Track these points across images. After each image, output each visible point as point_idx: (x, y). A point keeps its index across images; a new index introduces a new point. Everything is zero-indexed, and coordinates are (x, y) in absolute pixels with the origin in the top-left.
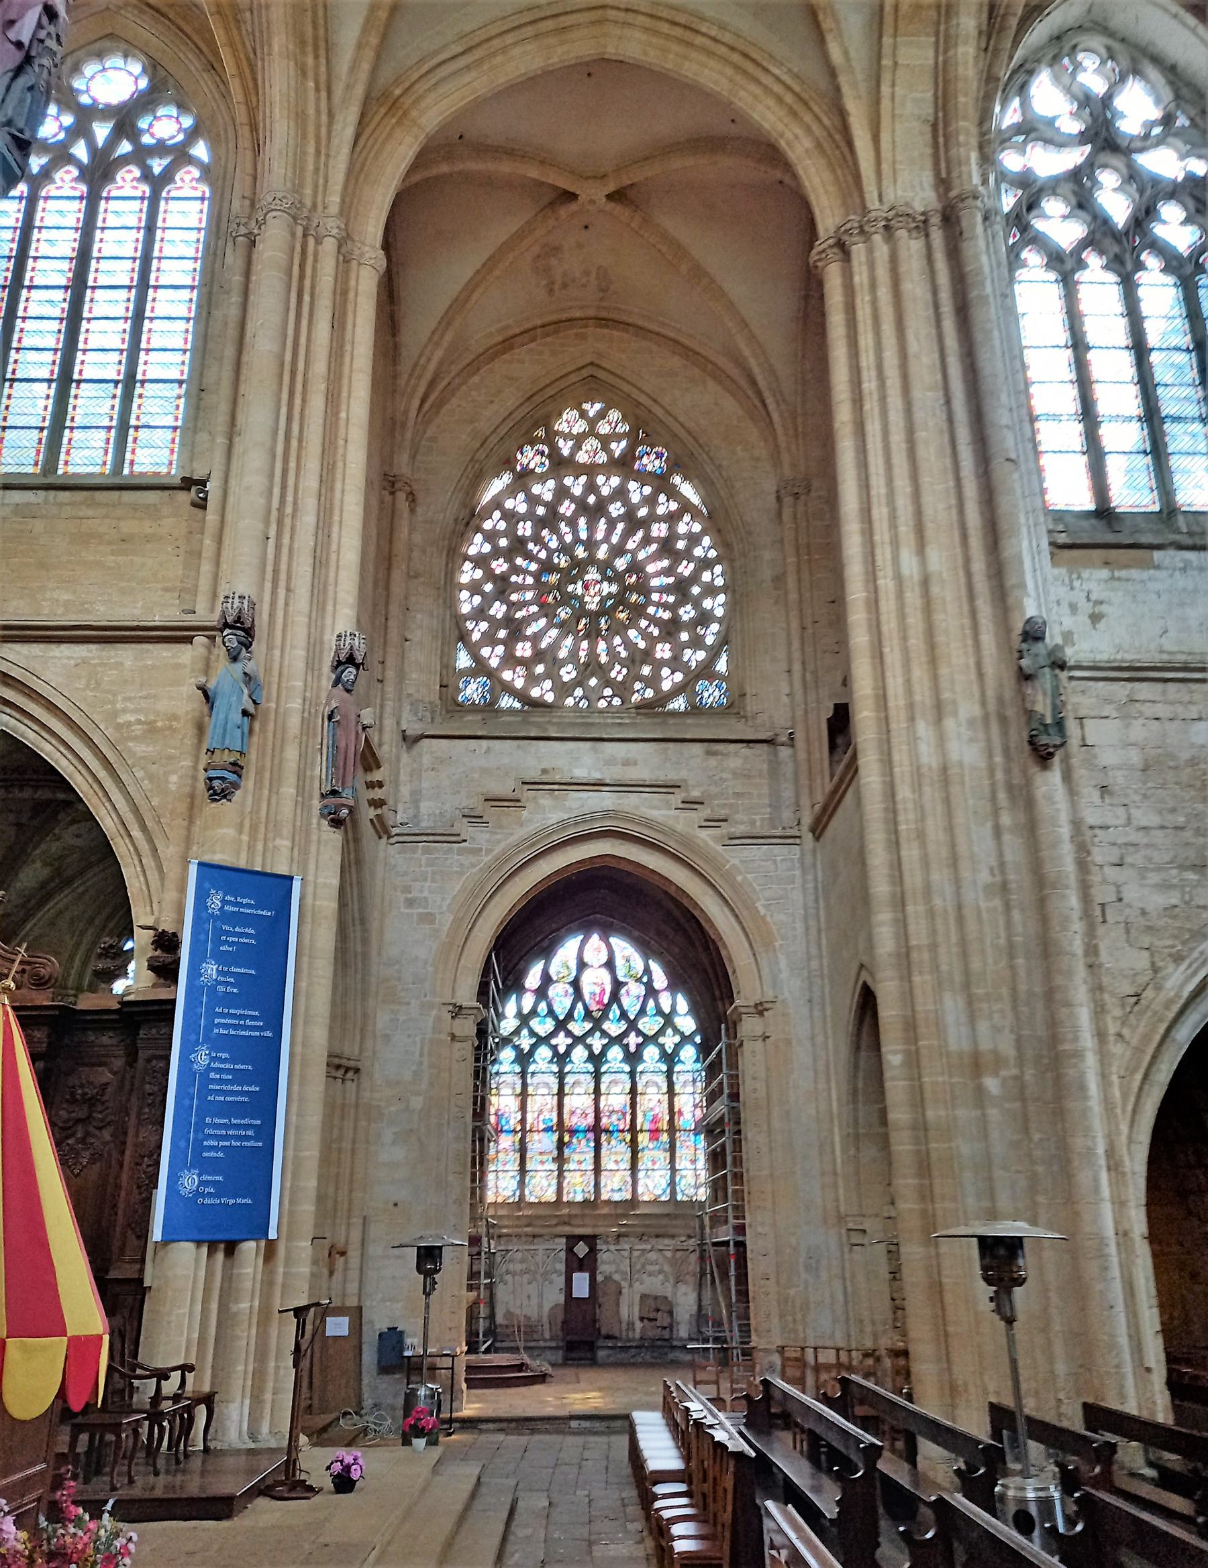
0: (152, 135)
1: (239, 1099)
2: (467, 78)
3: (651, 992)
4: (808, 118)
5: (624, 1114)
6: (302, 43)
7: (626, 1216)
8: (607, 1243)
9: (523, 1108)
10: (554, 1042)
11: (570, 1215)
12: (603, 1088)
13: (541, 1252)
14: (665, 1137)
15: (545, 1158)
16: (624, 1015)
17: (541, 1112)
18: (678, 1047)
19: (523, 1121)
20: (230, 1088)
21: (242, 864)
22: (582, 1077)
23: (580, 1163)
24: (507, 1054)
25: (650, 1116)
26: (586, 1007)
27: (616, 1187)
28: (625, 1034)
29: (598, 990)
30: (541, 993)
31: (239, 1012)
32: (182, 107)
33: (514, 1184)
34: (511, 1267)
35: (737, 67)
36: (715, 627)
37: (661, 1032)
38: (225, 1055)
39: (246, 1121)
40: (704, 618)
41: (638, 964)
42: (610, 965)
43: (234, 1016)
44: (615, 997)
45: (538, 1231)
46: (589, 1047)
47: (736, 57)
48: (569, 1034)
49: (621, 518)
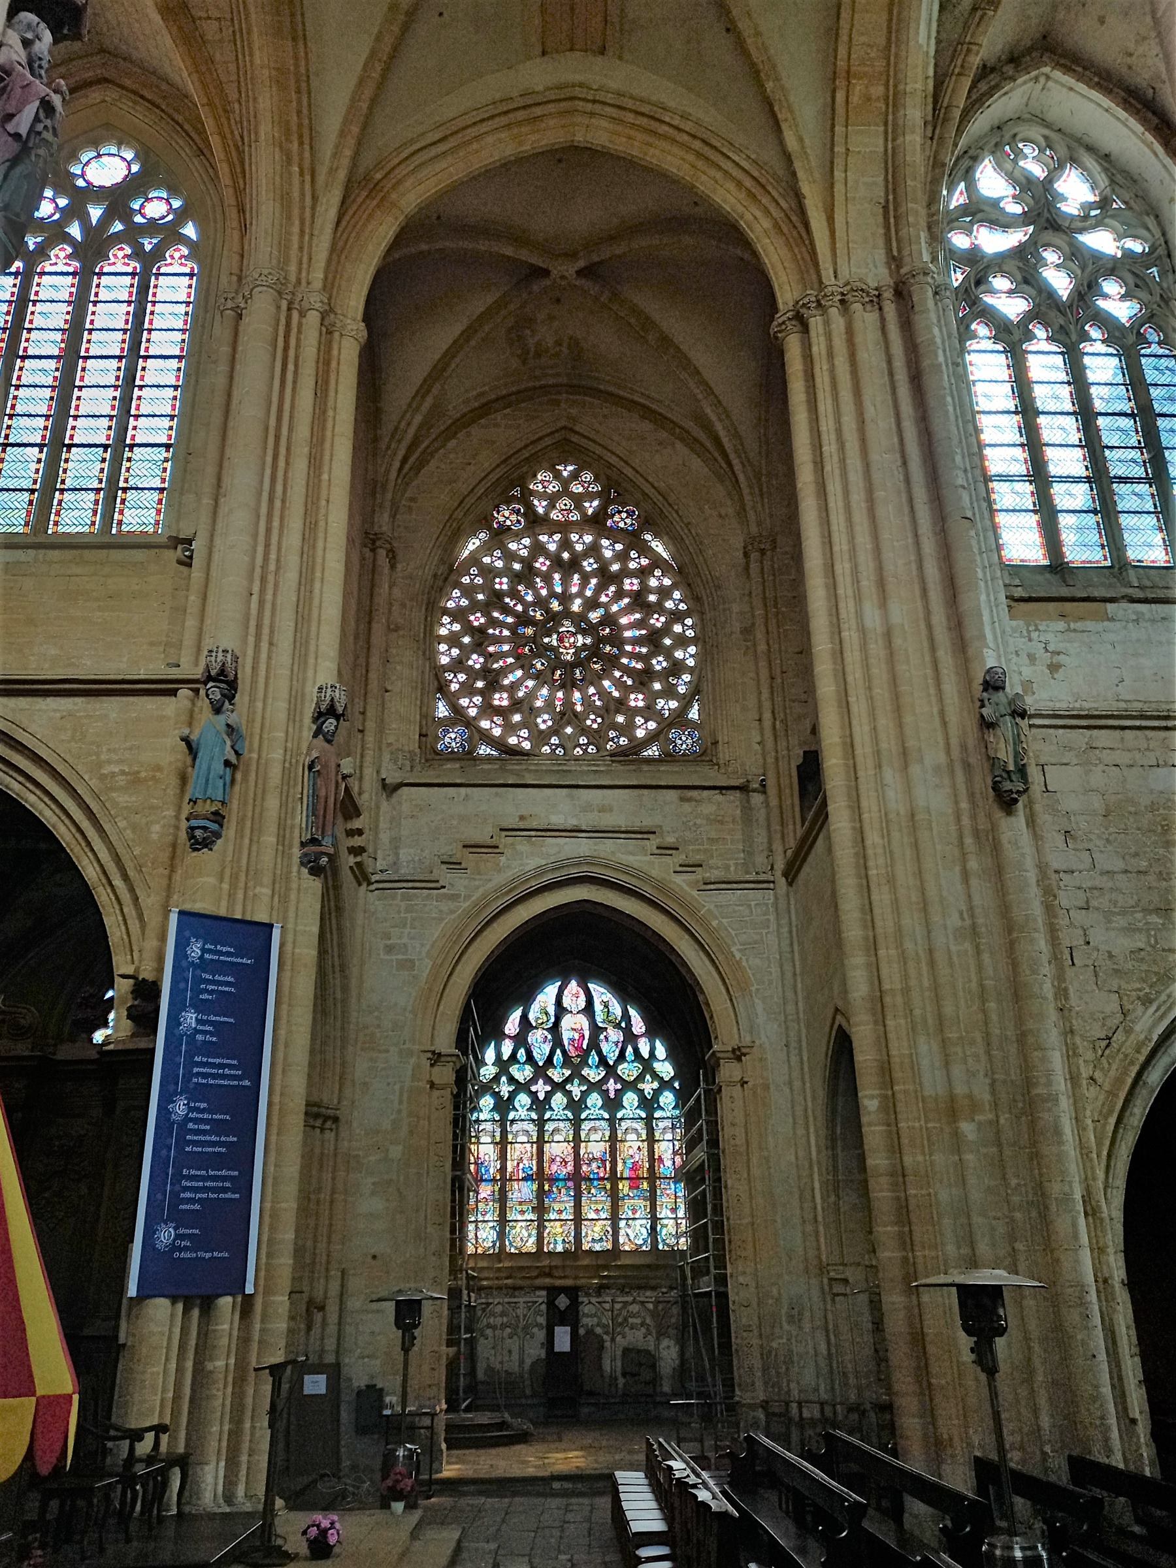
0: (144, 216)
1: (217, 1149)
2: (444, 165)
3: (630, 1037)
4: (765, 200)
5: (604, 1162)
6: (287, 132)
7: (606, 1267)
8: (588, 1295)
9: (503, 1157)
10: (533, 1089)
11: (550, 1267)
12: (583, 1135)
13: (521, 1305)
14: (645, 1185)
15: (525, 1208)
16: (603, 1061)
18: (657, 1093)
19: (503, 1169)
20: (208, 1138)
21: (222, 912)
22: (561, 1125)
23: (560, 1212)
24: (487, 1102)
26: (564, 1052)
27: (597, 1237)
28: (604, 1080)
29: (577, 1036)
30: (520, 1040)
31: (217, 1061)
32: (173, 191)
33: (493, 1235)
34: (491, 1320)
35: (699, 155)
36: (686, 677)
37: (640, 1078)
38: (203, 1105)
39: (224, 1173)
40: (676, 668)
41: (617, 1010)
42: (589, 1009)
43: (213, 1065)
44: (594, 1044)
45: (520, 1282)
46: (568, 1094)
47: (697, 145)
48: (548, 1080)
49: (594, 573)
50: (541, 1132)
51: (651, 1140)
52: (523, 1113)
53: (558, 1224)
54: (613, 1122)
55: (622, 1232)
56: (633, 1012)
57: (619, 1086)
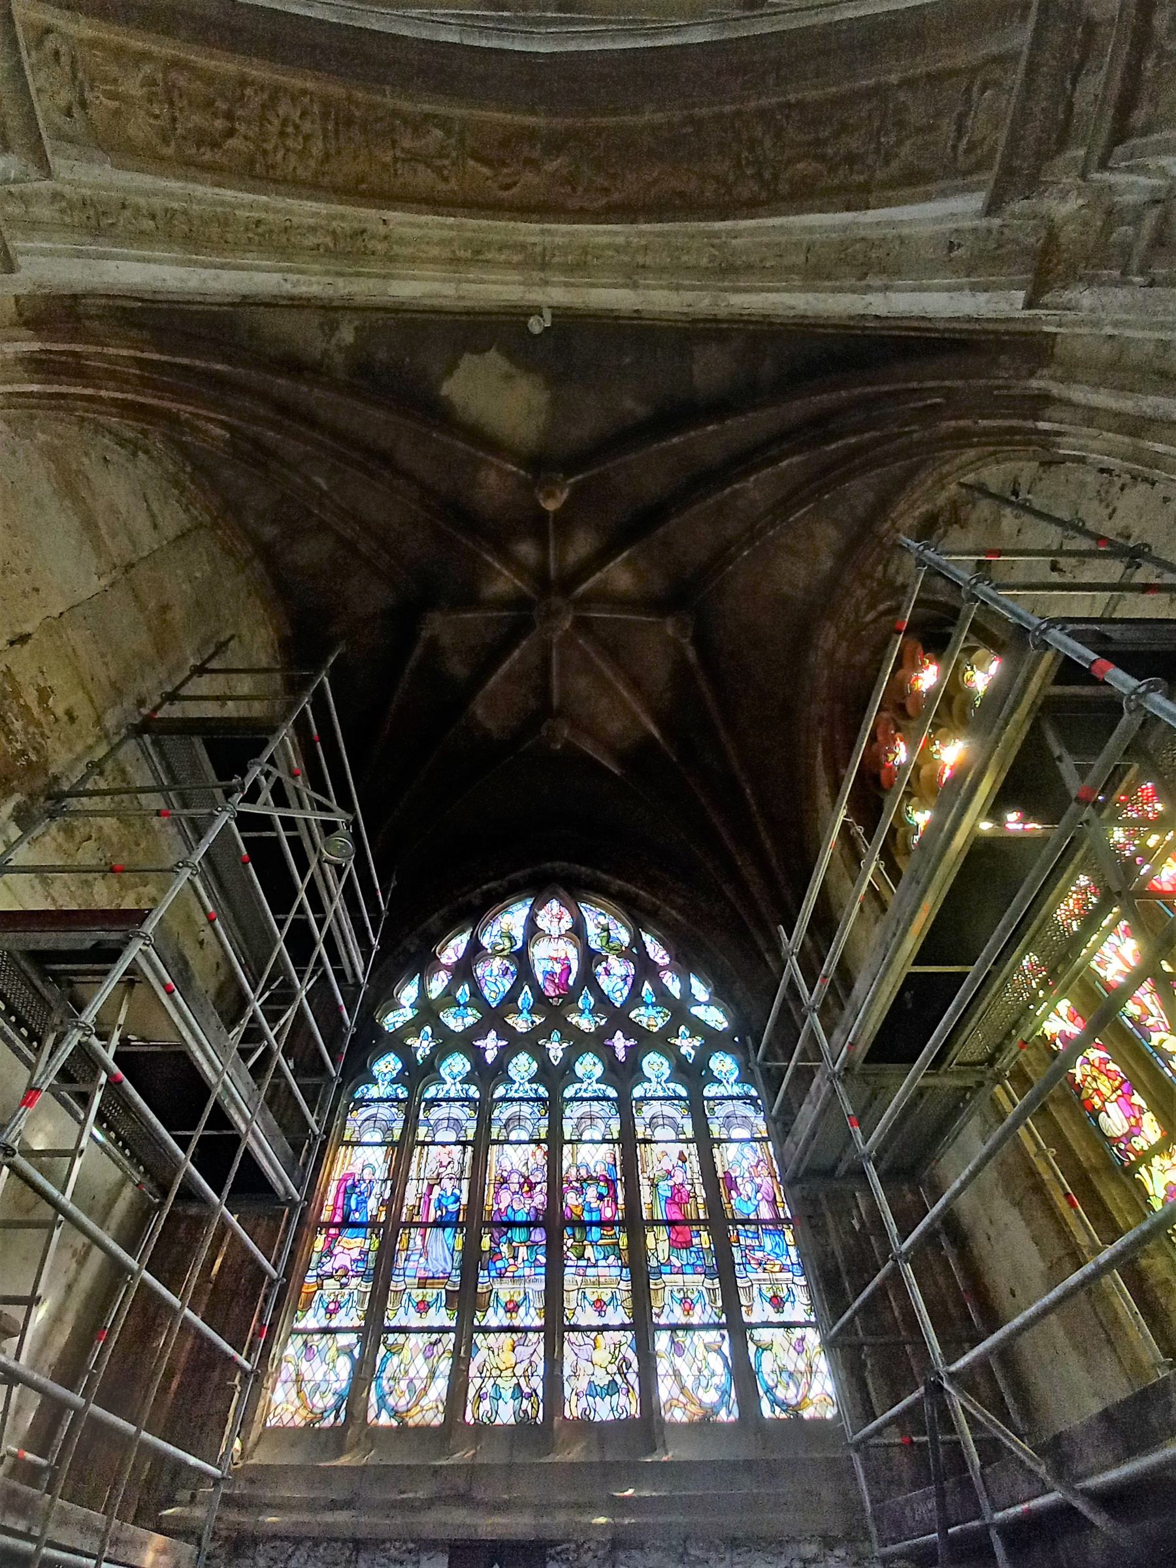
3: (646, 969)
5: (610, 1183)
7: (634, 1472)
9: (398, 1175)
11: (472, 1470)
14: (704, 1240)
15: (430, 1294)
16: (603, 1000)
17: (439, 1178)
18: (703, 1055)
19: (394, 1201)
22: (526, 1109)
24: (387, 1065)
25: (664, 1189)
29: (558, 968)
30: (464, 971)
37: (670, 1030)
41: (623, 936)
44: (588, 979)
48: (506, 1032)
50: (484, 1122)
51: (705, 1142)
52: (453, 1089)
53: (506, 1339)
54: (625, 1108)
55: (663, 1366)
56: (647, 938)
57: (632, 1042)
